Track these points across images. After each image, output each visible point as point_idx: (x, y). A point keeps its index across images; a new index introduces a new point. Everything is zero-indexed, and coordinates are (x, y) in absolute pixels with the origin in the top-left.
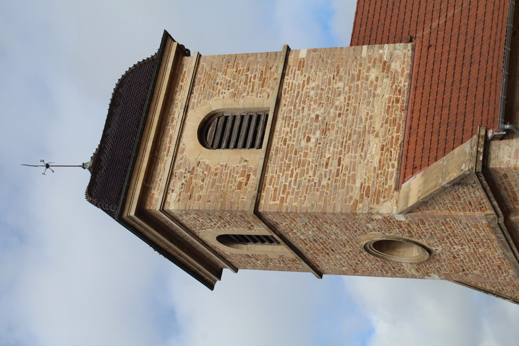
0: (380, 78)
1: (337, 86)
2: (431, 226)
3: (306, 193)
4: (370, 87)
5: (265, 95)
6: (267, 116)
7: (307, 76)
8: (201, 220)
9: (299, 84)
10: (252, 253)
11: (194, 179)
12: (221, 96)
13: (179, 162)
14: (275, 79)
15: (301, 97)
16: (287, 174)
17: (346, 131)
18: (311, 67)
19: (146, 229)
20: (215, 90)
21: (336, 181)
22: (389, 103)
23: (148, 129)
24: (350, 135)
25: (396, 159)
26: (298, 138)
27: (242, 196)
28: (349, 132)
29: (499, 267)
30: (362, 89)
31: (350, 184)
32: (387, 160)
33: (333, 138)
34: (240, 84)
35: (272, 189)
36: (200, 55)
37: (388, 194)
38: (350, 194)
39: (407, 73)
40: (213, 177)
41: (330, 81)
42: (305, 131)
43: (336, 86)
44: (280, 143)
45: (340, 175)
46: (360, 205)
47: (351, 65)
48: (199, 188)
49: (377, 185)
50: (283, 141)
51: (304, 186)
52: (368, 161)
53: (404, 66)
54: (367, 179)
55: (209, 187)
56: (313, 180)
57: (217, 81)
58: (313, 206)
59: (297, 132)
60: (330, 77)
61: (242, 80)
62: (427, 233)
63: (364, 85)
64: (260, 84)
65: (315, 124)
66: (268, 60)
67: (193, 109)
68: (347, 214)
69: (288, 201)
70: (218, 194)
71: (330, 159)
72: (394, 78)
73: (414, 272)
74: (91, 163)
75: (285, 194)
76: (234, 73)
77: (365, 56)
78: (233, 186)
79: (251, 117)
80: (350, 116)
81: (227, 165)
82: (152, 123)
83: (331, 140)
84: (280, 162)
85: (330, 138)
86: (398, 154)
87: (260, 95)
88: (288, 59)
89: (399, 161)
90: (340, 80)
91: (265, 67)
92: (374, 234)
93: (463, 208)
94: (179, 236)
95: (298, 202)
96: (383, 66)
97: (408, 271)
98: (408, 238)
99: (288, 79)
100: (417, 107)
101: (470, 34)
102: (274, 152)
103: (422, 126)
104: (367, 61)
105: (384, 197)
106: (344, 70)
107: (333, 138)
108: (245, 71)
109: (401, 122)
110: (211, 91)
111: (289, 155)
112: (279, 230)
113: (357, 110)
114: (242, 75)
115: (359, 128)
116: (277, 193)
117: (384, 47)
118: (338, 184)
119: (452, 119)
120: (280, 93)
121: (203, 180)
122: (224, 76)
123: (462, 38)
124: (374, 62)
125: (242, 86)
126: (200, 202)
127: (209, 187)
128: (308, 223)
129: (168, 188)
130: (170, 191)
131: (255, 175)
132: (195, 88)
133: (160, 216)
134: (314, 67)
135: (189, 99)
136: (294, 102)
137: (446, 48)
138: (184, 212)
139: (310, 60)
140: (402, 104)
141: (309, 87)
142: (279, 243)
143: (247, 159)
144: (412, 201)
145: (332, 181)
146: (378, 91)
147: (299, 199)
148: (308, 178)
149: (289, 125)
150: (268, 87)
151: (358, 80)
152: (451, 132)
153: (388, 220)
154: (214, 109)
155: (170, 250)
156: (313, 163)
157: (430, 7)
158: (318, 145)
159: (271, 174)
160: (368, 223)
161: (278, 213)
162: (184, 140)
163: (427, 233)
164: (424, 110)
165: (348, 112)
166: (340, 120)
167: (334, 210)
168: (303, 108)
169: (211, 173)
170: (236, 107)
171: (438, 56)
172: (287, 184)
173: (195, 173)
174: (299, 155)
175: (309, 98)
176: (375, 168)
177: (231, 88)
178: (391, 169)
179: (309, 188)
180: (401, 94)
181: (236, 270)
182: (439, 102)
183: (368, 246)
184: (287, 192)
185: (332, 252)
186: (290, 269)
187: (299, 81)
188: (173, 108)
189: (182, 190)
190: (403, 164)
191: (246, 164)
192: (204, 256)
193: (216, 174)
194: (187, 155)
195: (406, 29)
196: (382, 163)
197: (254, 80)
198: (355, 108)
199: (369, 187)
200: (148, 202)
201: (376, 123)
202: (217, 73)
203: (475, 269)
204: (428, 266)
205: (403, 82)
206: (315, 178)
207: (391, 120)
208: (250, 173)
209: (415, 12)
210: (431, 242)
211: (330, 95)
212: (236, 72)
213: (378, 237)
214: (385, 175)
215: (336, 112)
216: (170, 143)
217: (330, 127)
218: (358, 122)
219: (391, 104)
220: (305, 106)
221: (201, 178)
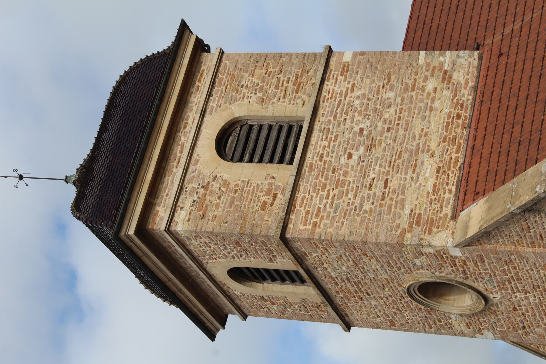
0: (439, 89)
1: (387, 97)
2: (492, 265)
3: (344, 218)
4: (427, 99)
5: (300, 102)
6: (301, 127)
7: (351, 83)
8: (212, 246)
9: (341, 91)
10: (269, 294)
11: (209, 195)
12: (246, 101)
13: (191, 175)
14: (313, 84)
15: (343, 106)
16: (323, 195)
17: (396, 148)
18: (357, 73)
19: (145, 254)
20: (239, 93)
21: (381, 205)
22: (448, 119)
23: (155, 134)
25: (453, 183)
27: (266, 218)
28: (399, 150)
30: (417, 102)
32: (443, 184)
33: (380, 155)
34: (270, 88)
35: (304, 212)
36: (223, 52)
38: (398, 221)
39: (472, 85)
40: (232, 194)
42: (346, 146)
43: (385, 96)
44: (315, 159)
45: (386, 199)
46: (408, 235)
47: (405, 73)
48: (214, 207)
49: (429, 213)
50: (319, 157)
51: (342, 209)
52: (420, 184)
53: (468, 77)
54: (418, 205)
55: (227, 206)
56: (353, 203)
57: (242, 83)
58: (351, 233)
59: (336, 146)
60: (379, 86)
61: (273, 83)
62: (486, 274)
63: (419, 97)
64: (294, 89)
65: (358, 138)
66: (305, 62)
67: (211, 114)
68: (392, 245)
69: (322, 226)
70: (237, 215)
71: (375, 180)
72: (456, 90)
73: (463, 328)
74: (77, 176)
75: (319, 218)
76: (263, 75)
77: (423, 63)
78: (255, 206)
79: (281, 127)
80: (401, 132)
81: (250, 182)
82: (160, 127)
83: (377, 158)
84: (314, 181)
85: (376, 156)
86: (456, 178)
87: (294, 102)
88: (329, 62)
89: (457, 186)
90: (391, 89)
91: (301, 70)
92: (422, 274)
93: (532, 243)
94: (181, 267)
95: (334, 228)
96: (443, 76)
97: (456, 326)
98: (461, 280)
99: (328, 85)
100: (482, 124)
102: (307, 169)
103: (487, 146)
104: (424, 69)
105: (438, 227)
106: (396, 78)
107: (380, 155)
108: (276, 73)
109: (462, 141)
110: (234, 94)
111: (325, 173)
112: (307, 263)
113: (410, 124)
114: (273, 78)
115: (412, 146)
116: (309, 217)
117: (445, 53)
118: (383, 209)
119: (526, 135)
120: (318, 100)
121: (219, 198)
122: (251, 78)
124: (433, 71)
125: (272, 91)
126: (215, 222)
127: (227, 206)
128: (343, 256)
129: (176, 205)
130: (178, 209)
131: (283, 194)
132: (214, 90)
133: (164, 239)
134: (360, 73)
135: (206, 102)
136: (335, 112)
137: (521, 56)
138: (194, 235)
139: (356, 64)
140: (464, 120)
141: (353, 96)
142: (303, 282)
143: (275, 175)
144: (473, 231)
145: (376, 206)
146: (437, 104)
147: (336, 224)
148: (347, 200)
149: (327, 138)
150: (304, 94)
151: (413, 90)
152: (523, 152)
154: (236, 116)
155: (169, 284)
156: (354, 183)
157: (503, 11)
158: (361, 163)
159: (304, 195)
160: (417, 257)
161: (309, 240)
162: (198, 150)
164: (491, 128)
165: (399, 127)
166: (389, 136)
168: (345, 119)
169: (230, 190)
170: (264, 114)
172: (322, 206)
173: (210, 189)
174: (337, 174)
175: (353, 108)
176: (428, 193)
177: (259, 92)
178: (447, 195)
179: (348, 212)
180: (464, 109)
181: (244, 316)
182: (510, 118)
183: (412, 290)
184: (321, 216)
185: (367, 296)
186: (311, 318)
187: (342, 88)
188: (186, 112)
189: (193, 208)
190: (462, 189)
191: (272, 181)
192: (208, 296)
193: (236, 191)
194: (201, 167)
195: (472, 35)
196: (437, 188)
197: (287, 85)
198: (407, 122)
199: (420, 214)
200: (151, 221)
201: (432, 141)
202: (242, 74)
203: (538, 326)
204: (481, 319)
205: (467, 96)
206: (356, 201)
207: (450, 138)
208: (277, 192)
209: (484, 17)
210: (490, 286)
211: (378, 106)
212: (266, 73)
213: (425, 277)
214: (441, 201)
215: (384, 126)
216: (181, 152)
217: (377, 142)
218: (410, 139)
219: (450, 120)
220: (348, 117)
221: (217, 195)
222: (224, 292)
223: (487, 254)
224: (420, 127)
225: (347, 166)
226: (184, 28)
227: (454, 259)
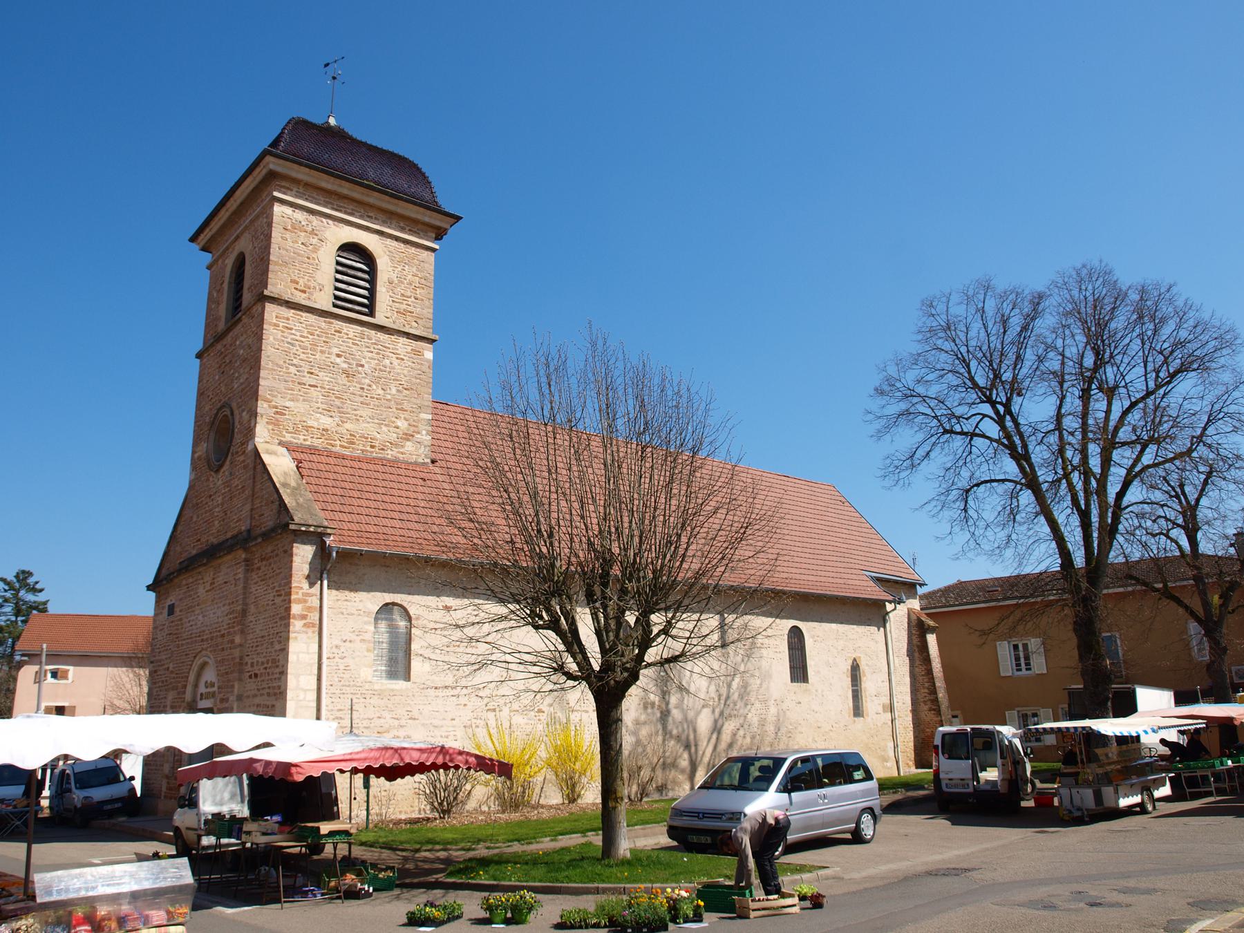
5: (389, 315)
9: (397, 349)
12: (390, 269)
24: (340, 398)
29: (199, 540)
31: (289, 396)
41: (398, 380)
43: (392, 386)
46: (265, 405)
56: (295, 358)
58: (268, 357)
63: (391, 414)
89: (310, 446)
90: (398, 391)
99: (403, 340)
115: (348, 407)
118: (290, 383)
121: (302, 244)
146: (384, 428)
162: (348, 229)
167: (263, 378)
172: (293, 332)
178: (302, 437)
181: (209, 268)
186: (207, 325)
193: (308, 258)
199: (285, 415)
205: (390, 454)
219: (369, 440)
222: (227, 248)
224: (364, 415)
226: (458, 218)
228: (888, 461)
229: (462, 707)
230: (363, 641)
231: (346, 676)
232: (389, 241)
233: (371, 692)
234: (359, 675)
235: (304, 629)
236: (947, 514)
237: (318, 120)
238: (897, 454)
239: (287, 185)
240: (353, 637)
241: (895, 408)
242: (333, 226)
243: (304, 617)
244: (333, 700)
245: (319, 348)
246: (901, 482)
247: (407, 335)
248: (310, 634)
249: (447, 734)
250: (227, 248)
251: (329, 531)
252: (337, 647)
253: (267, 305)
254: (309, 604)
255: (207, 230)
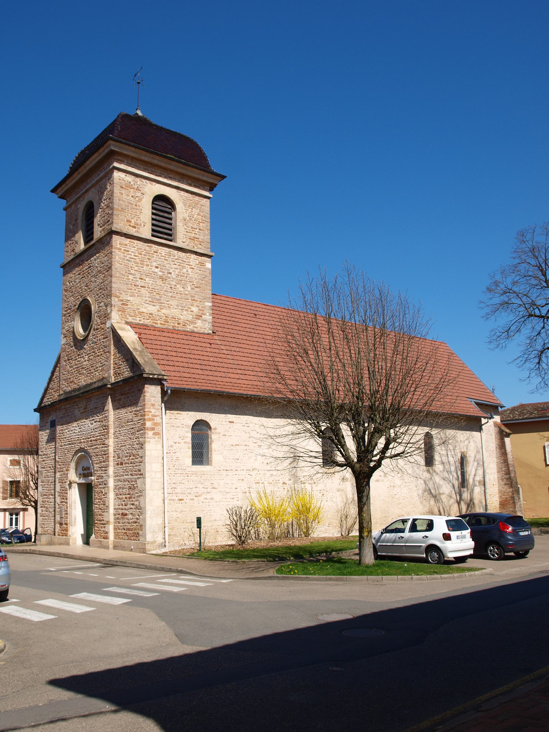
0: (192, 313)
6: (171, 241)
7: (195, 268)
9: (190, 262)
14: (194, 247)
16: (136, 253)
17: (161, 291)
21: (131, 284)
26: (158, 261)
31: (129, 294)
37: (123, 317)
40: (134, 204)
43: (188, 285)
46: (116, 299)
51: (128, 264)
56: (132, 269)
57: (194, 209)
58: (116, 269)
60: (193, 282)
62: (97, 340)
63: (188, 303)
65: (166, 272)
66: (205, 243)
68: (111, 291)
69: (119, 253)
79: (171, 230)
80: (170, 294)
89: (143, 324)
90: (192, 289)
92: (95, 307)
93: (116, 364)
97: (67, 325)
98: (93, 327)
99: (193, 256)
101: (219, 369)
103: (164, 339)
107: (158, 283)
109: (166, 326)
114: (197, 226)
116: (124, 246)
118: (130, 285)
121: (132, 197)
122: (196, 213)
123: (216, 364)
124: (202, 310)
126: (119, 194)
128: (103, 265)
137: (210, 354)
143: (145, 227)
144: (120, 333)
146: (185, 312)
147: (121, 260)
148: (133, 267)
152: (163, 357)
153: (107, 316)
154: (176, 206)
157: (232, 344)
160: (105, 304)
163: (97, 340)
165: (173, 293)
168: (176, 265)
170: (177, 221)
171: (205, 349)
172: (130, 253)
173: (137, 191)
178: (138, 319)
181: (65, 209)
182: (179, 350)
183: (86, 301)
185: (81, 277)
189: (126, 182)
193: (136, 206)
194: (148, 186)
195: (220, 329)
198: (175, 297)
199: (128, 305)
203: (70, 367)
205: (189, 328)
213: (94, 308)
219: (177, 320)
222: (79, 198)
223: (108, 340)
225: (152, 266)
226: (223, 177)
227: (105, 323)
228: (493, 333)
229: (241, 481)
230: (185, 442)
231: (177, 463)
232: (182, 193)
233: (191, 473)
234: (184, 462)
235: (154, 436)
236: (528, 365)
237: (131, 113)
238: (499, 328)
239: (121, 159)
240: (180, 440)
241: (497, 300)
242: (150, 185)
243: (153, 429)
244: (170, 477)
245: (145, 263)
246: (501, 346)
247: (196, 253)
248: (157, 439)
249: (233, 497)
250: (79, 198)
251: (165, 377)
252: (171, 446)
253: (114, 236)
254: (155, 421)
255: (64, 185)
